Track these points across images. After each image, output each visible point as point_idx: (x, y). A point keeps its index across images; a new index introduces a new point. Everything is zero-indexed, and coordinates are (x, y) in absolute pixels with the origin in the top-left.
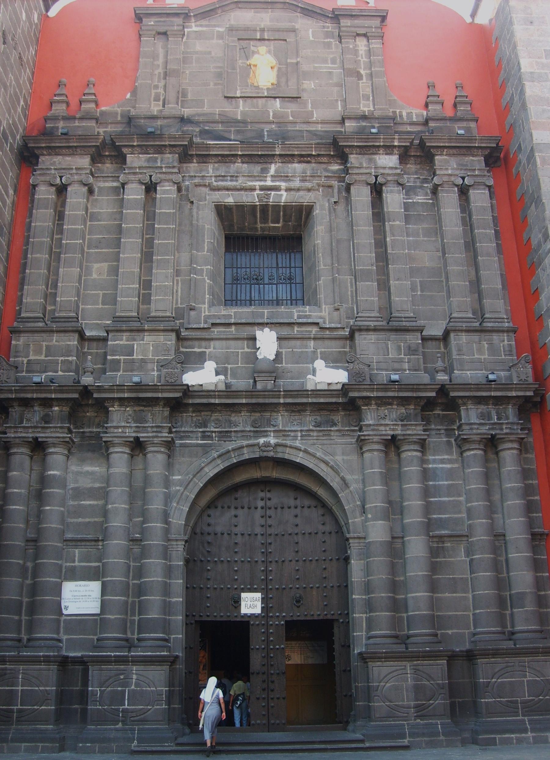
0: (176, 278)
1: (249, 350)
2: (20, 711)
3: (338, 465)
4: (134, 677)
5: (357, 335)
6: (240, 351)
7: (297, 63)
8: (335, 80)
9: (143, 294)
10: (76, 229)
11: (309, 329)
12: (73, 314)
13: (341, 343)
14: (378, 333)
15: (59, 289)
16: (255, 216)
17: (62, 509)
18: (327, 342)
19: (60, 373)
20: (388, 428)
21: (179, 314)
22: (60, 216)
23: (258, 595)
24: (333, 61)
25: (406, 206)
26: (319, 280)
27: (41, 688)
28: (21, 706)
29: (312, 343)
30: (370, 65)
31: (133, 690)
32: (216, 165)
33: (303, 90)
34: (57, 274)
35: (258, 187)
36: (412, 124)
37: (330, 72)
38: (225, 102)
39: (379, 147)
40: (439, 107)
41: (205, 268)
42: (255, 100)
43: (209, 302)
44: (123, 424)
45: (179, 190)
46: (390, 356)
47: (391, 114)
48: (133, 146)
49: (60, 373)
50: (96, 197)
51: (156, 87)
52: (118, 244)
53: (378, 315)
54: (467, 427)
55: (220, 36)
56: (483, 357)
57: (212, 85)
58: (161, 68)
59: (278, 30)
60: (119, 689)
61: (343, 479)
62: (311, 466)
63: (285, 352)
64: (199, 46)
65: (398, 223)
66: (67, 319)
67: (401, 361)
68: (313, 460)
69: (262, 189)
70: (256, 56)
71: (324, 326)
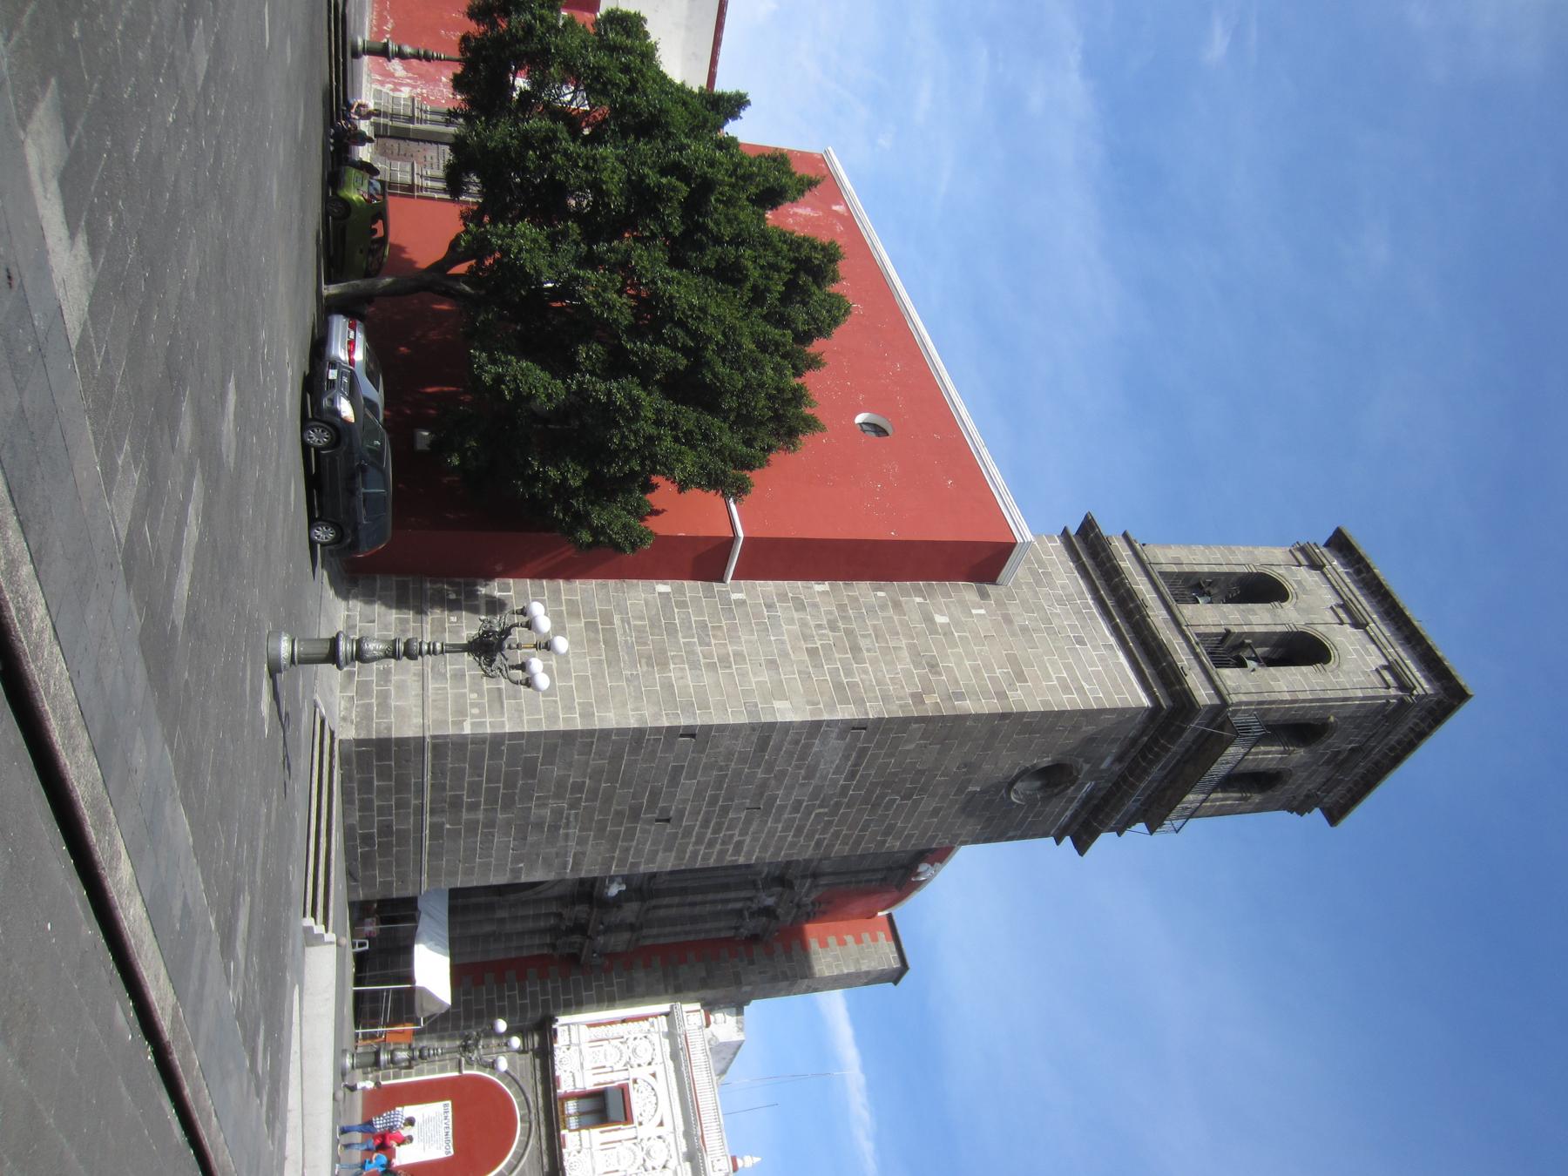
61: (540, 892)
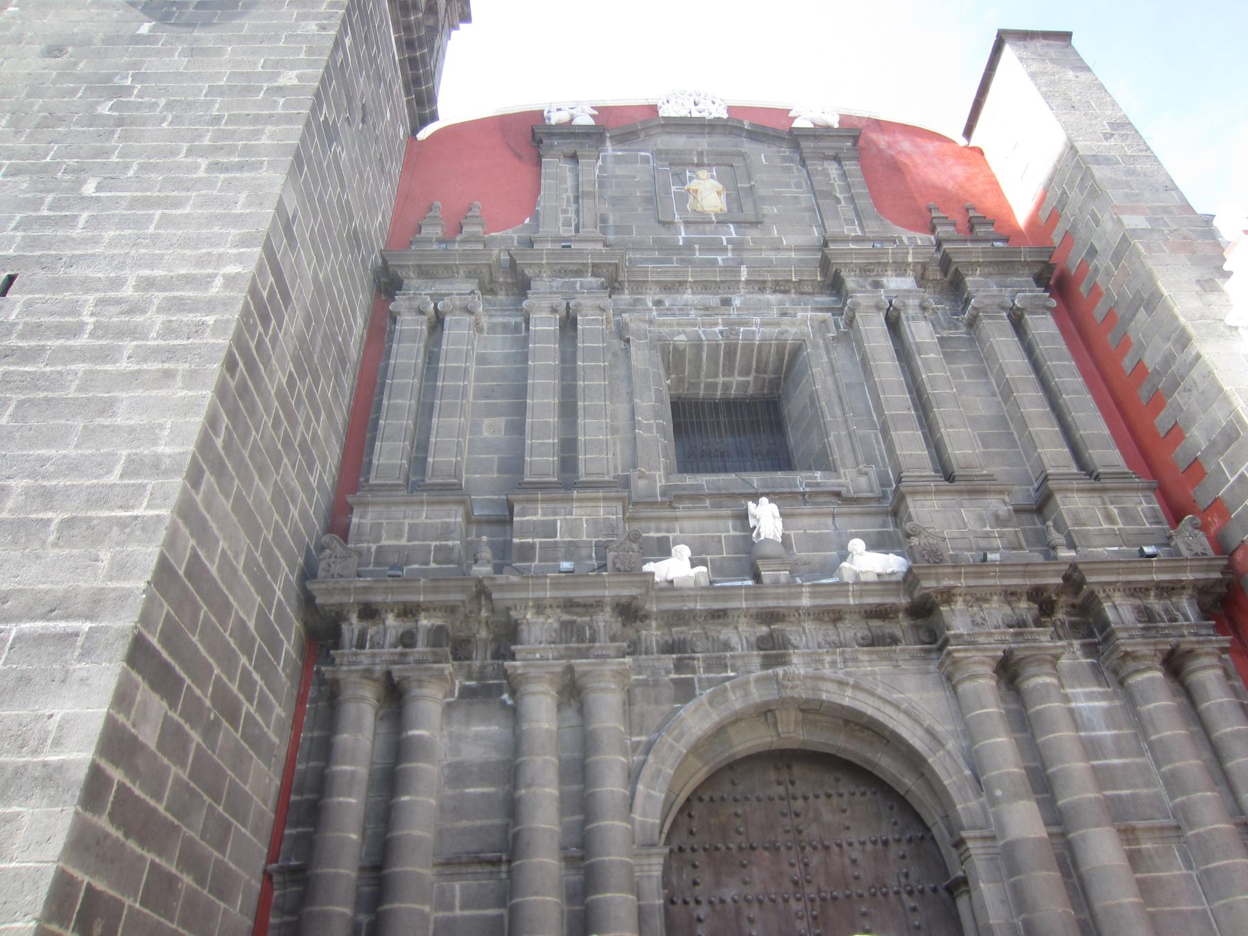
1: (738, 533)
6: (723, 535)
7: (751, 187)
14: (943, 497)
16: (717, 365)
19: (433, 565)
24: (798, 186)
33: (763, 215)
37: (796, 197)
49: (433, 565)
54: (1125, 635)
57: (640, 209)
59: (721, 154)
61: (930, 732)
62: (870, 711)
63: (795, 534)
65: (932, 355)
67: (987, 536)
68: (870, 700)
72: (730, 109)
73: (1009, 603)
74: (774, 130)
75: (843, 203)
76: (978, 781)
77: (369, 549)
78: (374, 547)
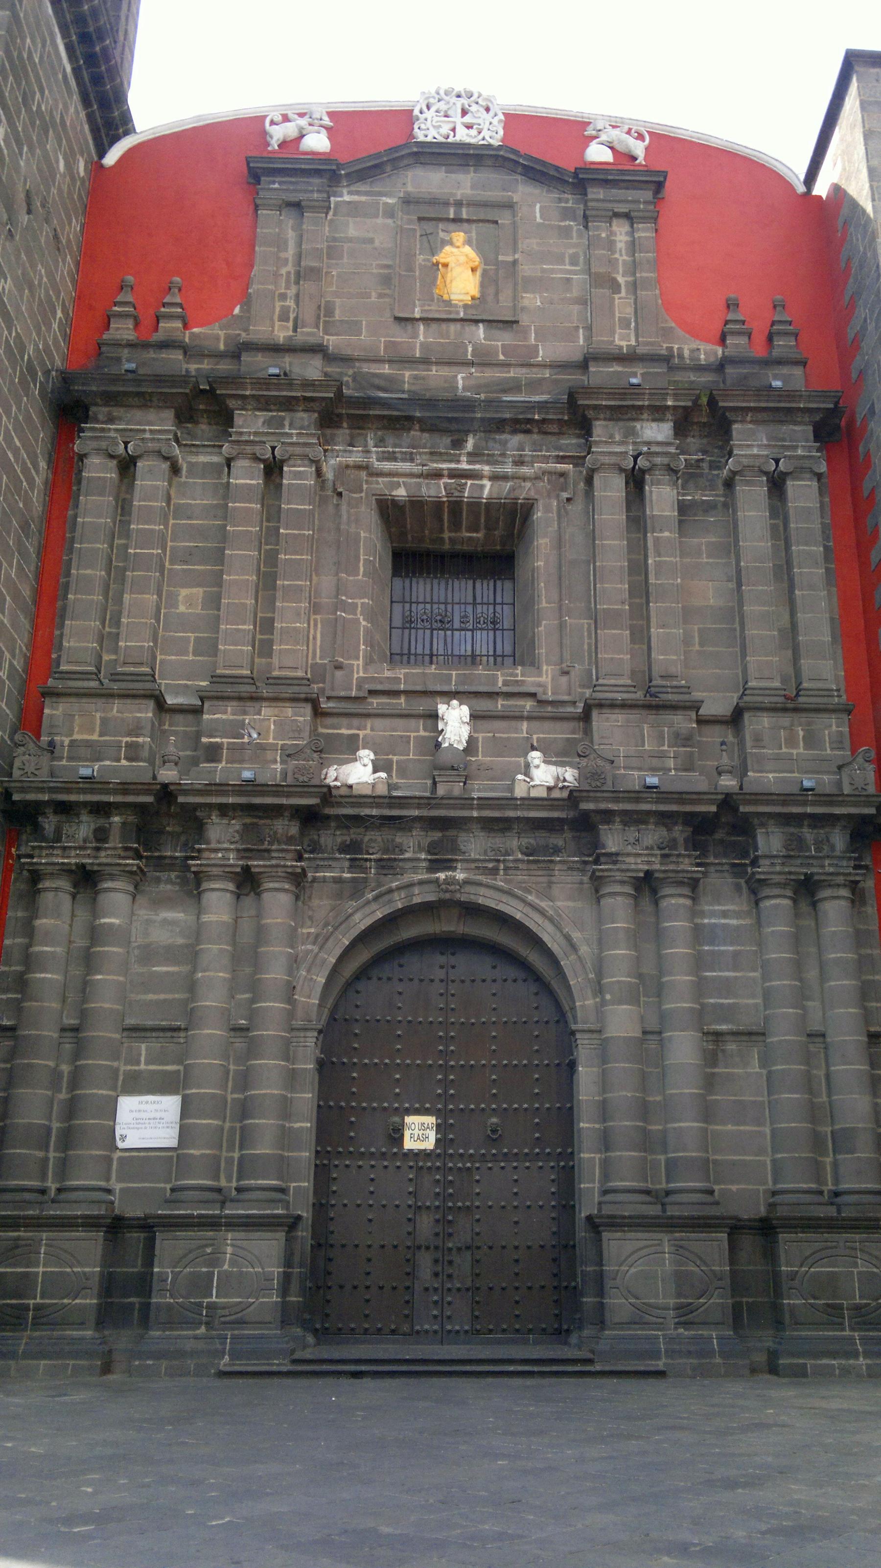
0: (313, 617)
1: (427, 734)
2: (38, 1308)
3: (559, 915)
4: (229, 1249)
5: (595, 714)
6: (412, 734)
7: (515, 263)
8: (575, 293)
9: (261, 641)
10: (152, 530)
11: (520, 702)
12: (146, 669)
13: (572, 725)
14: (629, 711)
15: (123, 630)
16: (441, 520)
17: (121, 979)
18: (548, 725)
20: (639, 861)
21: (319, 672)
22: (124, 507)
23: (431, 1120)
25: (683, 508)
26: (539, 625)
27: (75, 1270)
28: (42, 1298)
29: (525, 725)
30: (633, 268)
31: (226, 1271)
32: (380, 433)
33: (523, 309)
34: (119, 601)
35: (446, 473)
36: (700, 368)
37: (568, 280)
38: (396, 329)
39: (641, 408)
40: (743, 341)
41: (359, 602)
42: (444, 326)
43: (365, 657)
44: (226, 846)
45: (319, 473)
46: (646, 747)
47: (664, 352)
48: (244, 397)
49: (124, 762)
50: (183, 479)
51: (283, 297)
52: (219, 556)
53: (629, 682)
54: (767, 862)
55: (390, 213)
56: (795, 752)
57: (374, 298)
58: (290, 264)
59: (485, 205)
60: (204, 1270)
61: (568, 938)
62: (518, 916)
63: (483, 738)
64: (353, 229)
65: (667, 534)
66: (137, 677)
68: (520, 906)
69: (454, 474)
70: (448, 249)
71: (544, 697)
72: (513, 120)
73: (665, 825)
74: (557, 168)
75: (623, 293)
76: (599, 983)
77: (62, 742)
78: (67, 742)
